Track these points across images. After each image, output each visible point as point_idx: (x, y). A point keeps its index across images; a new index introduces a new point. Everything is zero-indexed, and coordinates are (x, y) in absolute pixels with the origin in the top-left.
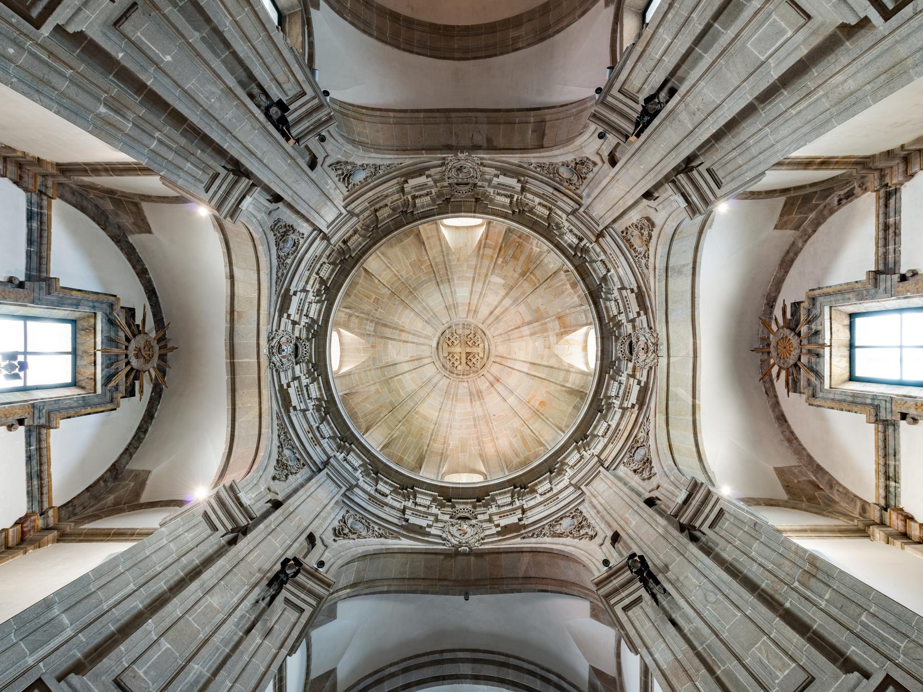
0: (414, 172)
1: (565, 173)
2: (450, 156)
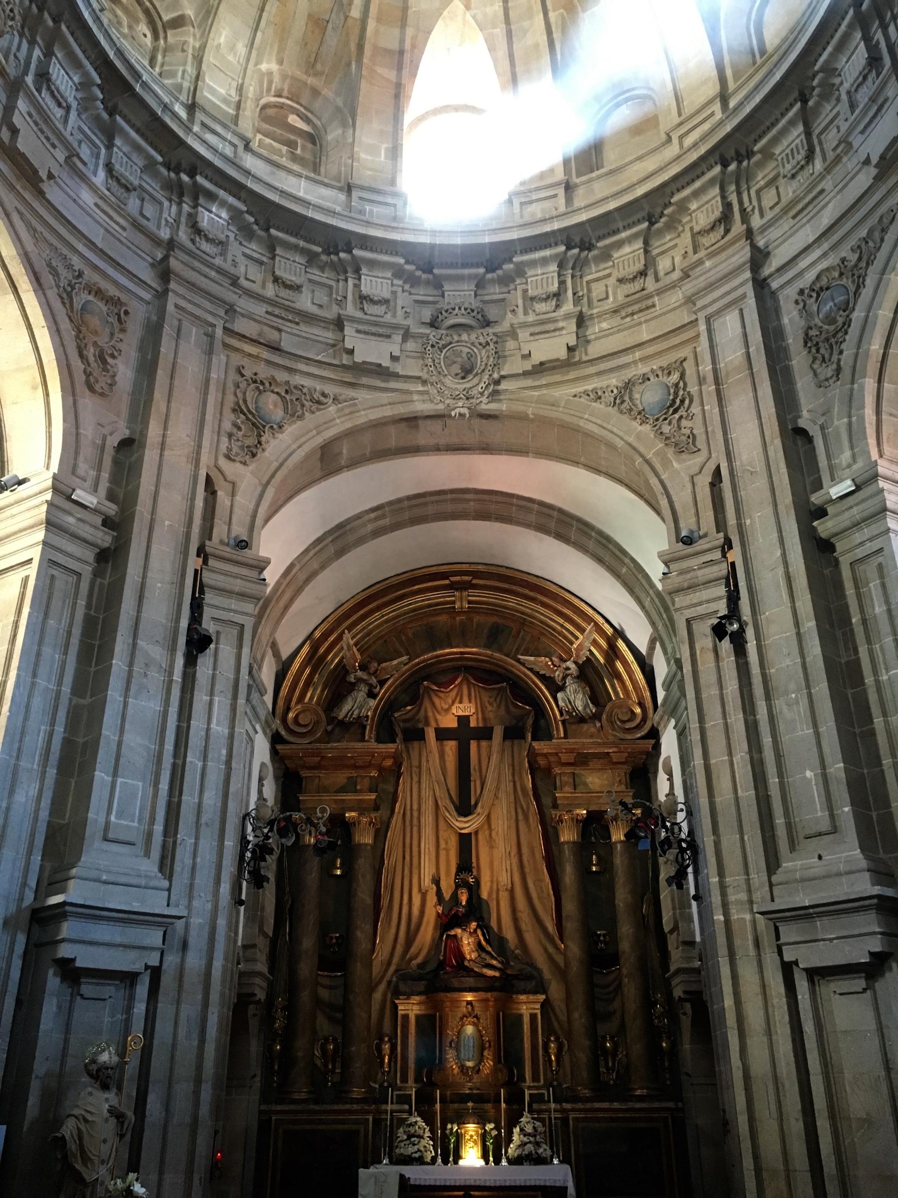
0: (554, 368)
1: (271, 404)
2: (486, 406)
